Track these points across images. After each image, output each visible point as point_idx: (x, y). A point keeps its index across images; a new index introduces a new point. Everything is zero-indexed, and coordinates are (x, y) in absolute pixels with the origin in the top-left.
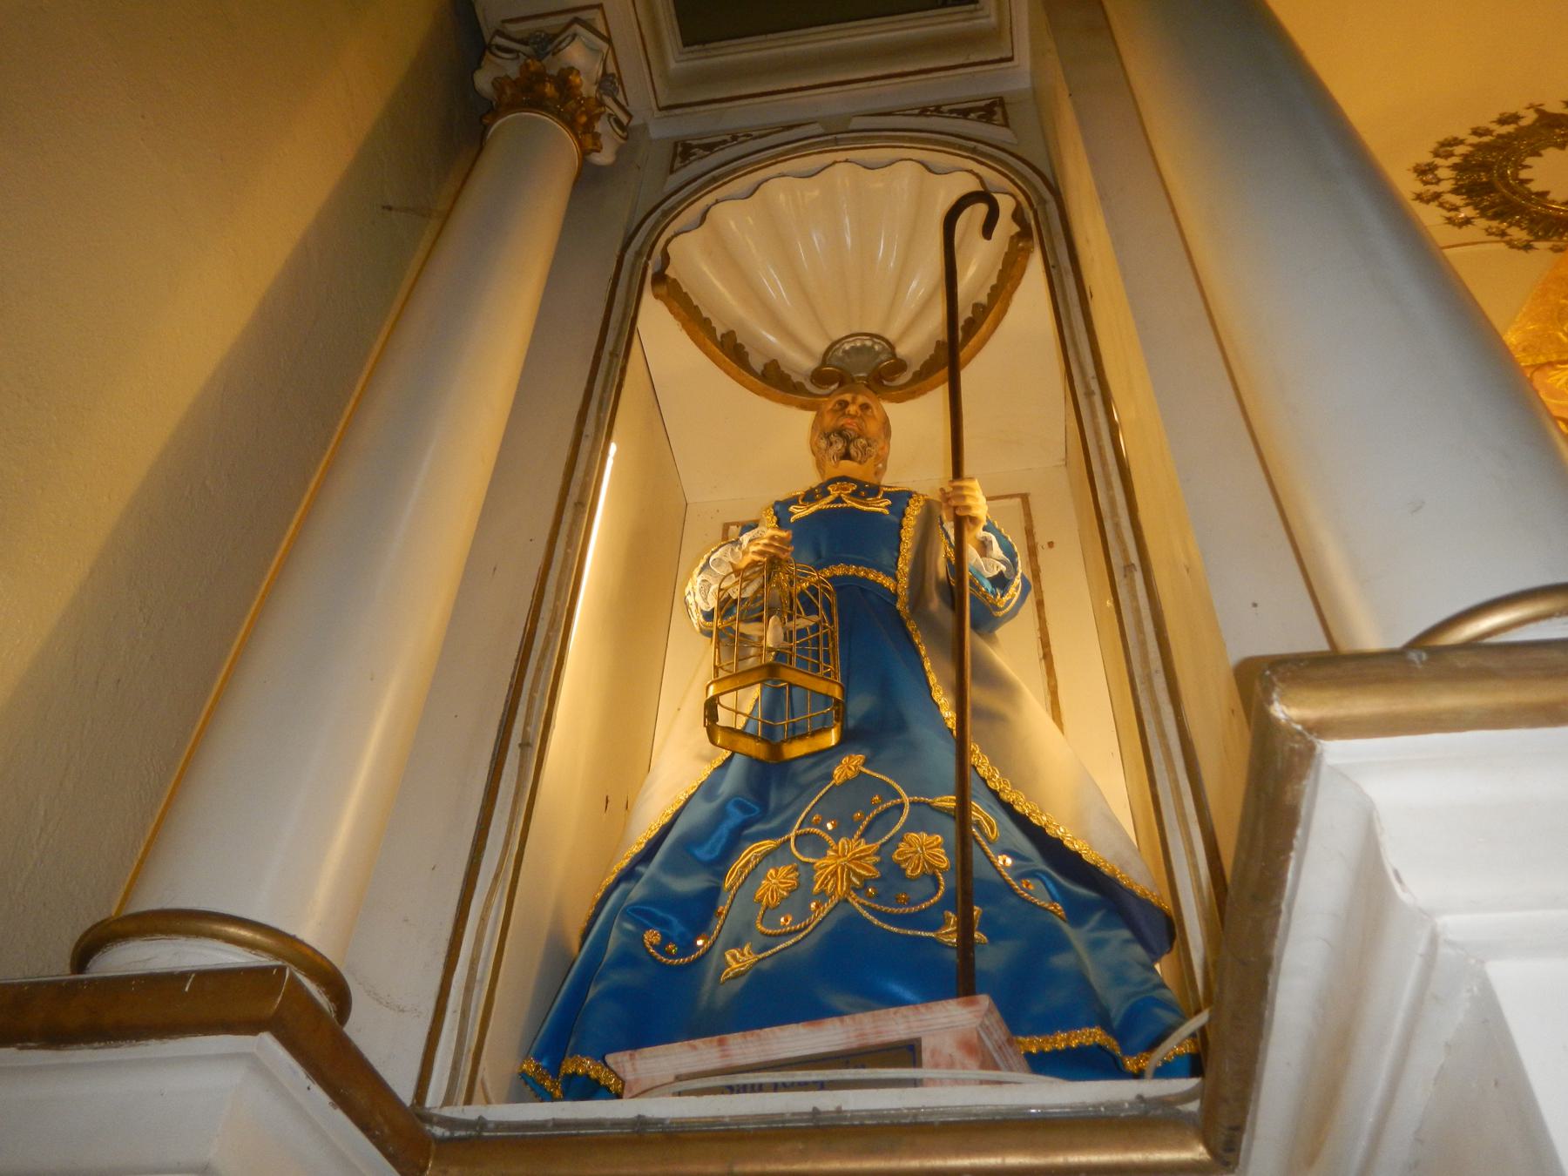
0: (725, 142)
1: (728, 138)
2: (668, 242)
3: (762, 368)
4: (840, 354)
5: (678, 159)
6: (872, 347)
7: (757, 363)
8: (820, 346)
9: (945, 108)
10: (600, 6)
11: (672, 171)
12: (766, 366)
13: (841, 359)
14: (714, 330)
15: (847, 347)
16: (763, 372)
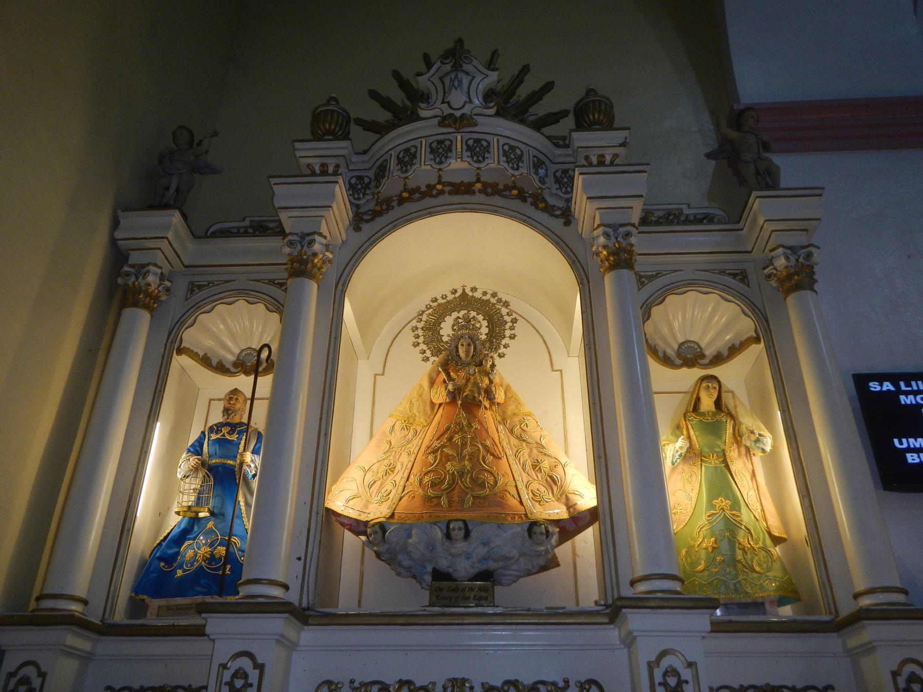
1: (206, 283)
2: (182, 334)
3: (216, 364)
4: (243, 355)
5: (189, 293)
6: (253, 354)
7: (214, 364)
8: (237, 351)
9: (276, 282)
10: (160, 249)
11: (186, 300)
12: (218, 363)
13: (243, 357)
14: (199, 355)
15: (246, 352)
16: (216, 366)
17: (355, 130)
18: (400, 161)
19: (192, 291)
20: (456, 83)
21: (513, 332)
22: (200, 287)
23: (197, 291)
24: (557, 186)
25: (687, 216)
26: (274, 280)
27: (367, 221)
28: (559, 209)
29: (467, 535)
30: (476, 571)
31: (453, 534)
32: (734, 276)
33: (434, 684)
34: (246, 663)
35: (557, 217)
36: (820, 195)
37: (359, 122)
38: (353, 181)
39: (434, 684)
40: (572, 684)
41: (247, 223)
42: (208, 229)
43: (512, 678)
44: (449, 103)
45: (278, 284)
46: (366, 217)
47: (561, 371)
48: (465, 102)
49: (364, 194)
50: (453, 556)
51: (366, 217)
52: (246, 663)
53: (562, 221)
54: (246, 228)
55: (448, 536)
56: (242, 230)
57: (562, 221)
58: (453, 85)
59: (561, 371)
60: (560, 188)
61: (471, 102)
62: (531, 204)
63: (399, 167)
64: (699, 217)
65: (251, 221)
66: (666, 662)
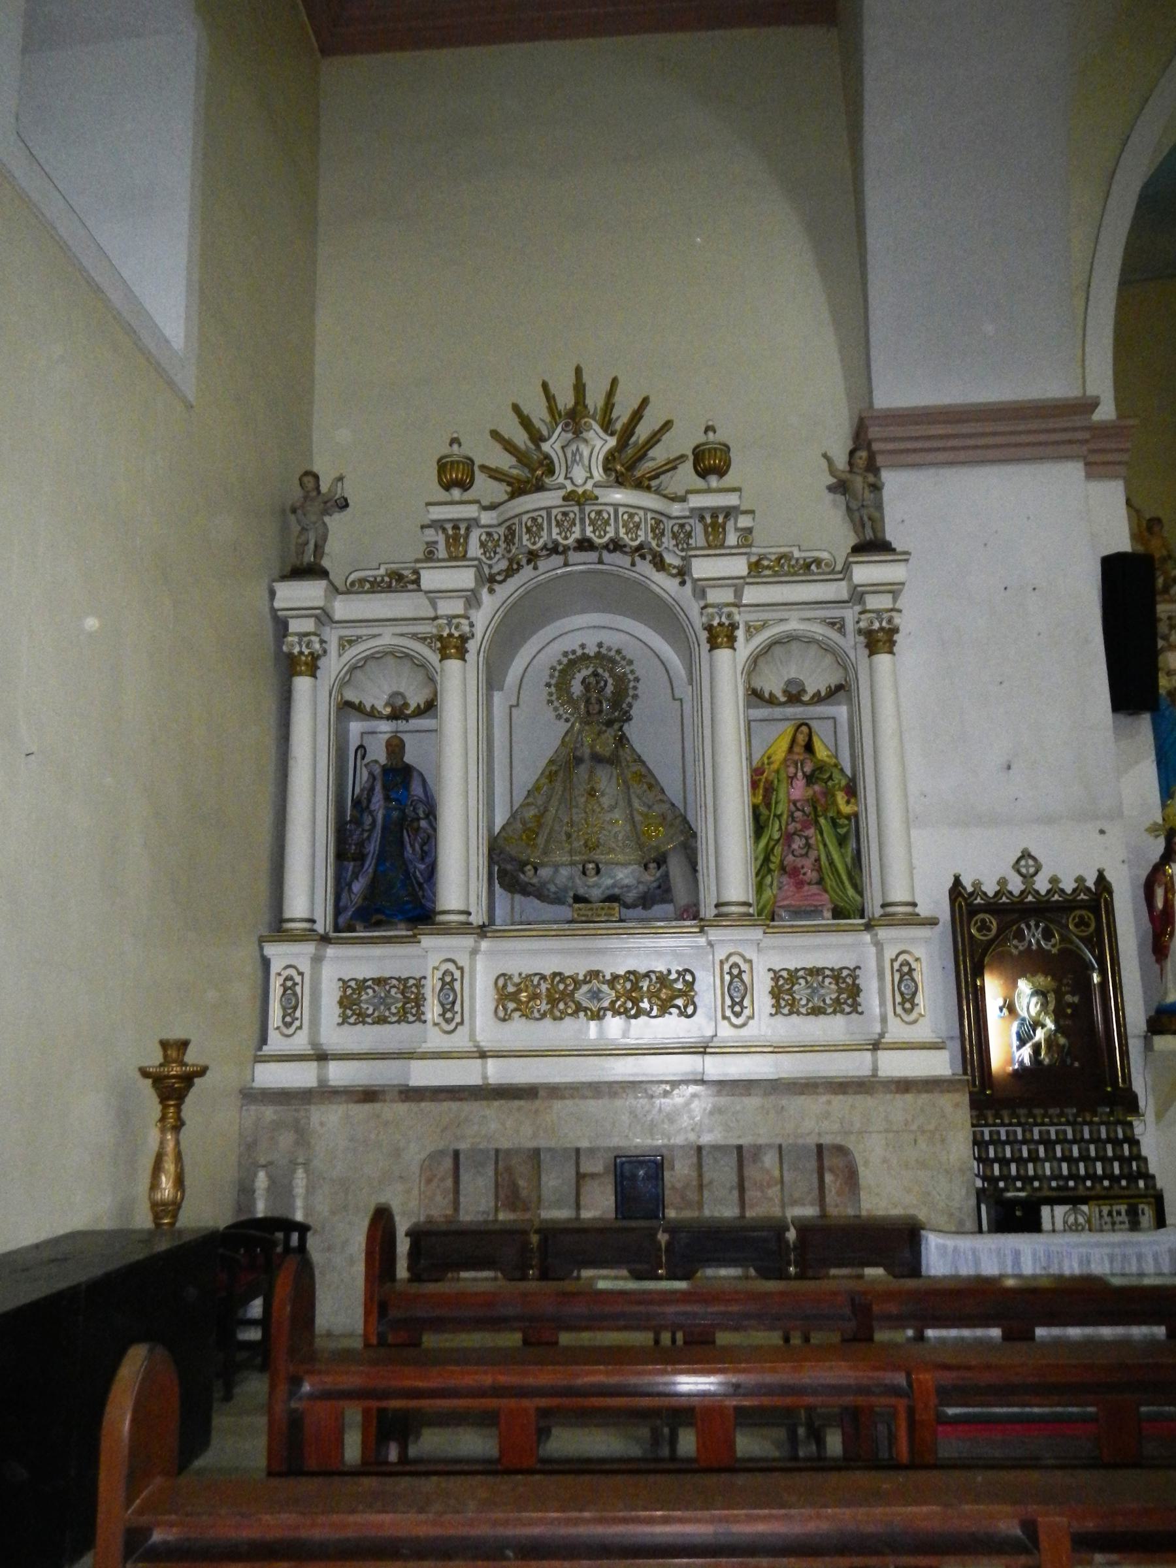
0: (354, 641)
9: (420, 636)
11: (340, 655)
17: (480, 478)
18: (529, 530)
19: (344, 647)
20: (578, 458)
21: (636, 684)
22: (350, 642)
23: (348, 646)
24: (674, 542)
25: (797, 560)
26: (417, 634)
27: (500, 582)
28: (675, 567)
29: (598, 871)
30: (604, 896)
31: (588, 872)
32: (833, 624)
33: (578, 974)
34: (451, 967)
35: (674, 576)
36: (906, 560)
37: (483, 468)
38: (484, 537)
39: (578, 974)
40: (673, 972)
41: (382, 571)
42: (347, 579)
43: (632, 969)
44: (571, 479)
45: (421, 638)
46: (499, 578)
47: (681, 700)
48: (587, 479)
49: (495, 553)
50: (589, 887)
51: (499, 578)
52: (451, 967)
53: (678, 580)
54: (382, 577)
55: (584, 873)
56: (379, 579)
57: (678, 580)
58: (575, 460)
59: (681, 700)
60: (677, 545)
61: (592, 477)
62: (650, 562)
63: (527, 536)
64: (808, 560)
65: (387, 570)
66: (733, 959)
